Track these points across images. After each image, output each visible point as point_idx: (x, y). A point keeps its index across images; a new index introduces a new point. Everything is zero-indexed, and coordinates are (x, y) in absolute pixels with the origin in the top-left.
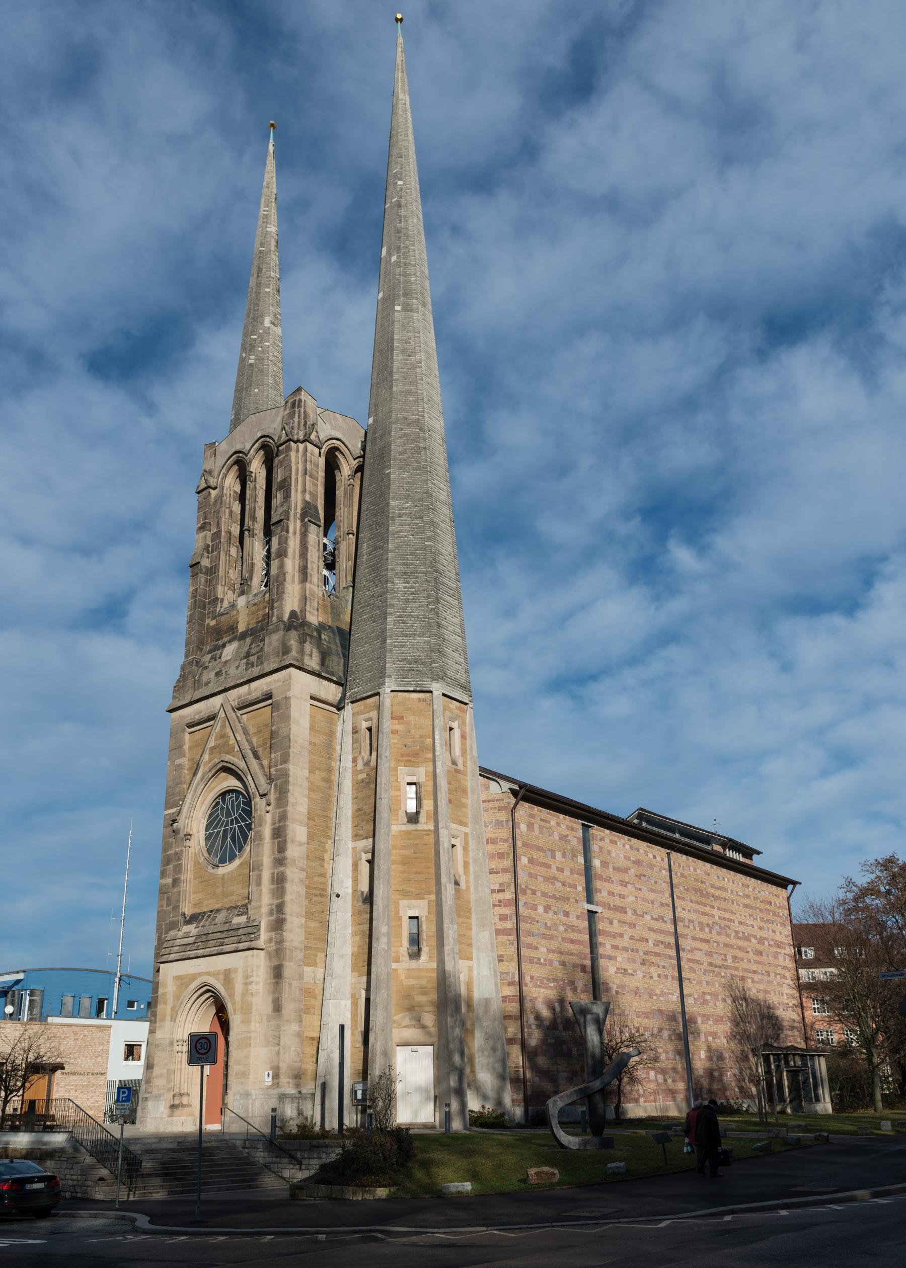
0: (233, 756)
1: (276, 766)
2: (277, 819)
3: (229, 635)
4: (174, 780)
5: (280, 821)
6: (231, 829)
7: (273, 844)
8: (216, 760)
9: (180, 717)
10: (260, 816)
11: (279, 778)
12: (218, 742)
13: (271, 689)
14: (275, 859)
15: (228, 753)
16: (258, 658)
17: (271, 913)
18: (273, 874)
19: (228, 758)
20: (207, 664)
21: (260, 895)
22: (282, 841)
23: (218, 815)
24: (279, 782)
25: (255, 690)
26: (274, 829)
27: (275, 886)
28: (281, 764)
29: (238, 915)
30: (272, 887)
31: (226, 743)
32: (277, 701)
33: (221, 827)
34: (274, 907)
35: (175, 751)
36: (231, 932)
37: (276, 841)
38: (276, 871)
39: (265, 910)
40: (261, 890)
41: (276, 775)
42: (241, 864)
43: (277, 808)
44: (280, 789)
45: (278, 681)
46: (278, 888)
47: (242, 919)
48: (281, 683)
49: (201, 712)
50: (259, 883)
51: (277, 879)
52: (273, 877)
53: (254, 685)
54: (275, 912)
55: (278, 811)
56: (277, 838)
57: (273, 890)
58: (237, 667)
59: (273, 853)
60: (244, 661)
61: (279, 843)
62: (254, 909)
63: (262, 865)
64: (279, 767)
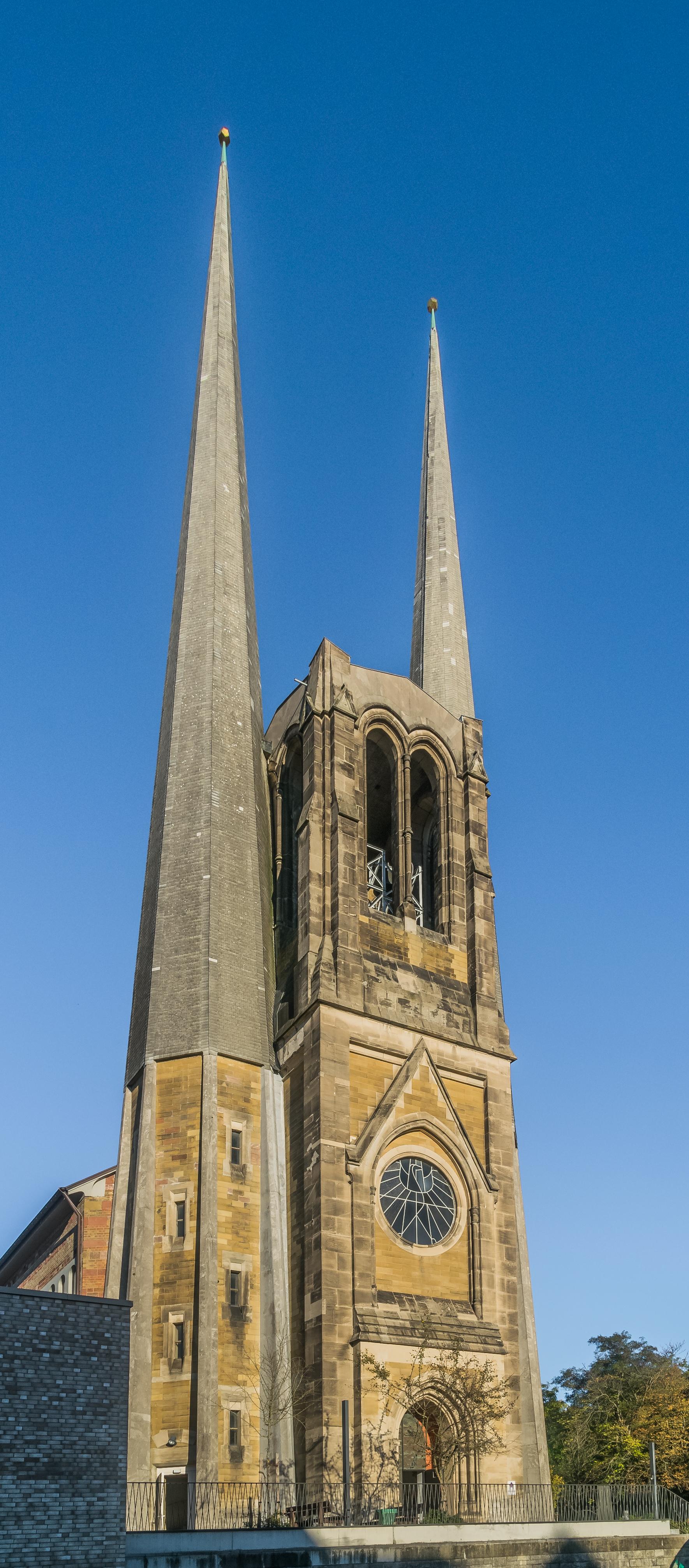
0: (444, 1123)
1: (499, 1163)
2: (503, 1223)
3: (394, 956)
4: (335, 1102)
5: (507, 1226)
6: (419, 1206)
7: (500, 1248)
8: (417, 1115)
9: (337, 1020)
10: (487, 1210)
11: (503, 1179)
12: (419, 1093)
13: (486, 1072)
14: (503, 1264)
15: (437, 1116)
16: (465, 1022)
17: (503, 1320)
18: (503, 1280)
19: (435, 1120)
20: (373, 974)
21: (494, 1299)
22: (511, 1248)
23: (397, 1181)
24: (503, 1182)
25: (463, 1059)
26: (500, 1232)
27: (506, 1294)
28: (504, 1164)
29: (459, 1311)
30: (502, 1293)
31: (432, 1101)
32: (494, 1089)
33: (404, 1196)
34: (506, 1315)
35: (332, 1064)
36: (465, 1329)
37: (504, 1246)
38: (506, 1278)
39: (498, 1315)
40: (495, 1293)
41: (498, 1174)
42: (447, 1254)
43: (502, 1211)
44: (504, 1191)
45: (494, 1067)
46: (509, 1297)
47: (471, 1318)
48: (498, 1072)
49: (378, 1036)
50: (491, 1285)
51: (508, 1287)
52: (503, 1284)
53: (461, 1051)
54: (507, 1321)
55: (504, 1214)
56: (504, 1242)
57: (504, 1297)
58: (435, 1014)
59: (502, 1259)
60: (445, 1013)
61: (507, 1249)
62: (487, 1311)
63: (494, 1266)
64: (501, 1166)
